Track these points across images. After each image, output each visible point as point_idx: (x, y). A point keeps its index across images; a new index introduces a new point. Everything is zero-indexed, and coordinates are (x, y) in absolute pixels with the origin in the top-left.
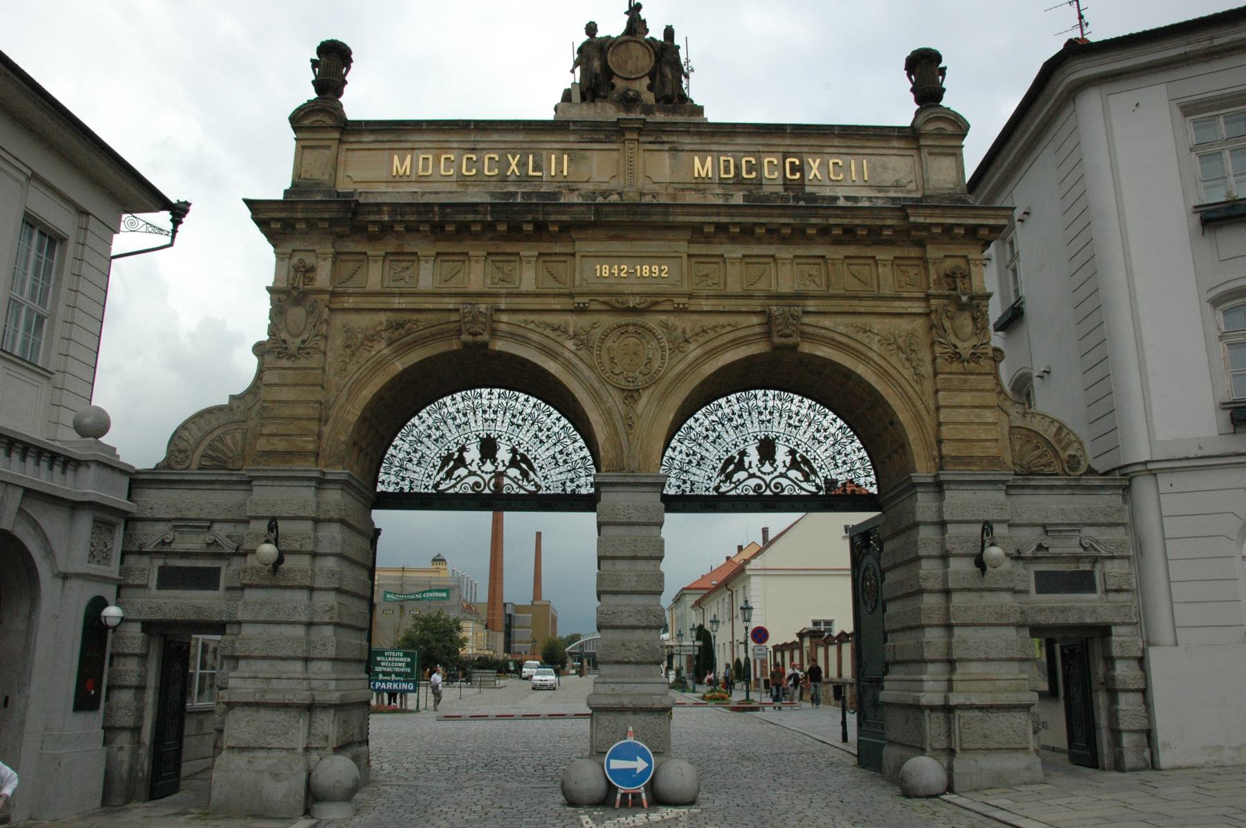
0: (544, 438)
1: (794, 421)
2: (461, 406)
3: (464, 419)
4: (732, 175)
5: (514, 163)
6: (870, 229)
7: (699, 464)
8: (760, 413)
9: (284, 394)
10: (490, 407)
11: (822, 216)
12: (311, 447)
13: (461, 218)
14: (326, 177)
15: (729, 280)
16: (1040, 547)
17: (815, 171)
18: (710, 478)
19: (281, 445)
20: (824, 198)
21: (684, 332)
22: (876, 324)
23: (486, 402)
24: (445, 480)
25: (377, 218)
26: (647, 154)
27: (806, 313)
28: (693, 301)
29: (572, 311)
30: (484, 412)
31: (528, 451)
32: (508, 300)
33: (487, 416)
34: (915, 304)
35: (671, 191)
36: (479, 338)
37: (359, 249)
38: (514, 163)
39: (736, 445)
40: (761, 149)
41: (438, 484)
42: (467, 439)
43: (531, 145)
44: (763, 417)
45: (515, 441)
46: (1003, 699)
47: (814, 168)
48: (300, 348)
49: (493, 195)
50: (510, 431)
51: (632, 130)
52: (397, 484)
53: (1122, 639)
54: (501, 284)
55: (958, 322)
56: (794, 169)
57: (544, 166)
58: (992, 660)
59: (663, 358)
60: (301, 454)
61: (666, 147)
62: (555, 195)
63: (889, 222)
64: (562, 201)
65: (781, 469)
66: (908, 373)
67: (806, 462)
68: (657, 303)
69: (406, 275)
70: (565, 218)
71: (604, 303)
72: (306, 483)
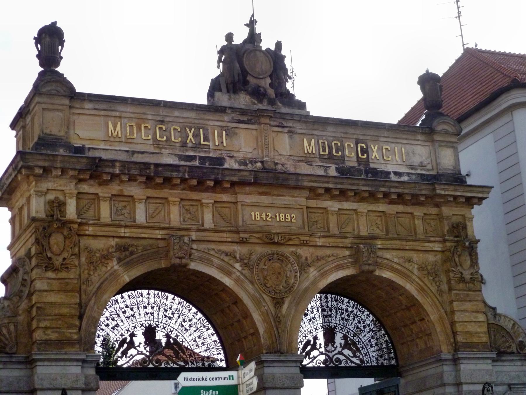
0: (187, 327)
1: (345, 316)
2: (128, 303)
3: (132, 313)
4: (327, 153)
5: (191, 134)
6: (413, 195)
9: (52, 298)
10: (149, 304)
11: (387, 187)
12: (75, 337)
13: (168, 174)
14: (62, 133)
15: (331, 225)
17: (375, 153)
19: (54, 336)
20: (383, 172)
21: (306, 259)
22: (415, 256)
23: (146, 300)
24: (121, 357)
25: (111, 170)
26: (274, 134)
28: (311, 239)
29: (237, 243)
31: (177, 336)
32: (198, 233)
33: (147, 310)
34: (437, 245)
36: (184, 261)
37: (92, 190)
38: (191, 134)
39: (310, 332)
42: (135, 327)
43: (201, 121)
44: (326, 313)
45: (168, 329)
47: (375, 153)
48: (62, 264)
49: (181, 158)
50: (164, 321)
55: (463, 258)
56: (364, 151)
57: (211, 137)
59: (295, 277)
60: (70, 343)
61: (286, 130)
62: (220, 161)
63: (424, 192)
64: (226, 166)
65: (339, 349)
66: (434, 289)
67: (354, 344)
68: (290, 239)
69: (125, 211)
70: (235, 179)
71: (258, 238)
72: (75, 363)
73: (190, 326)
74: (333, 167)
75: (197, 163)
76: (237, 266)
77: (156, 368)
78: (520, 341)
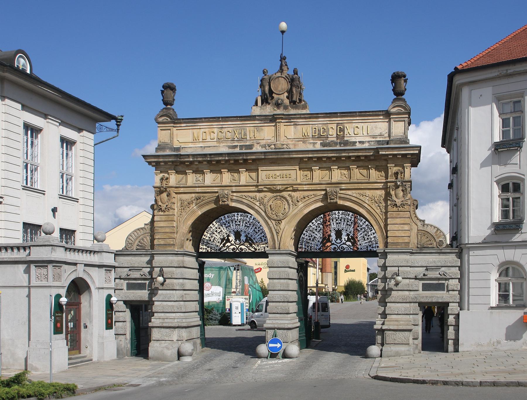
7: (313, 240)
8: (337, 220)
9: (162, 224)
12: (172, 243)
13: (217, 159)
16: (424, 275)
18: (317, 245)
20: (351, 142)
22: (368, 192)
27: (341, 189)
30: (236, 222)
31: (252, 236)
35: (293, 142)
40: (328, 122)
41: (221, 248)
46: (401, 327)
51: (279, 118)
52: (206, 249)
53: (453, 308)
54: (233, 181)
58: (400, 314)
61: (292, 124)
62: (250, 147)
64: (254, 150)
66: (378, 211)
70: (254, 157)
73: (259, 231)
74: (319, 142)
75: (237, 150)
76: (258, 204)
77: (240, 253)
78: (440, 241)
